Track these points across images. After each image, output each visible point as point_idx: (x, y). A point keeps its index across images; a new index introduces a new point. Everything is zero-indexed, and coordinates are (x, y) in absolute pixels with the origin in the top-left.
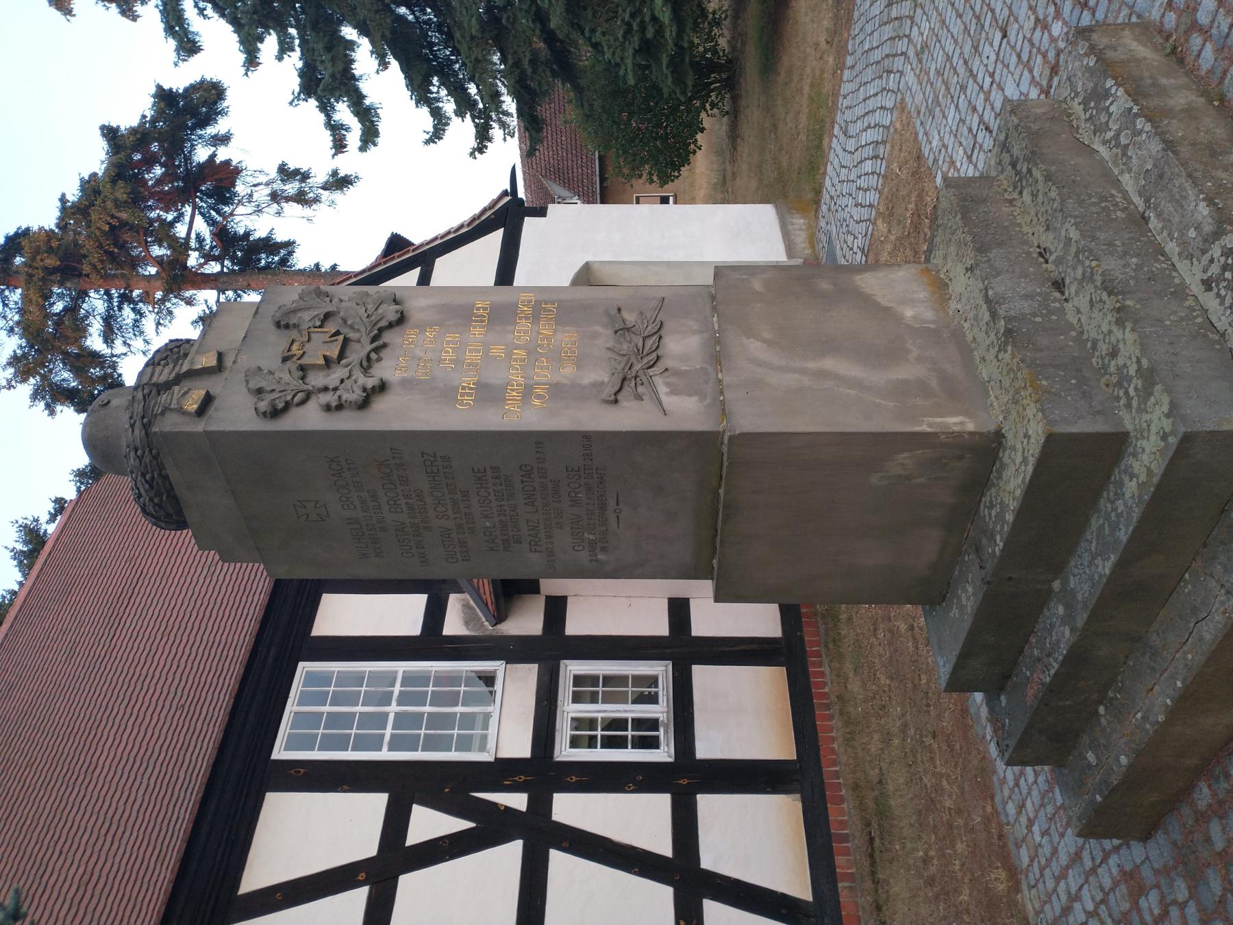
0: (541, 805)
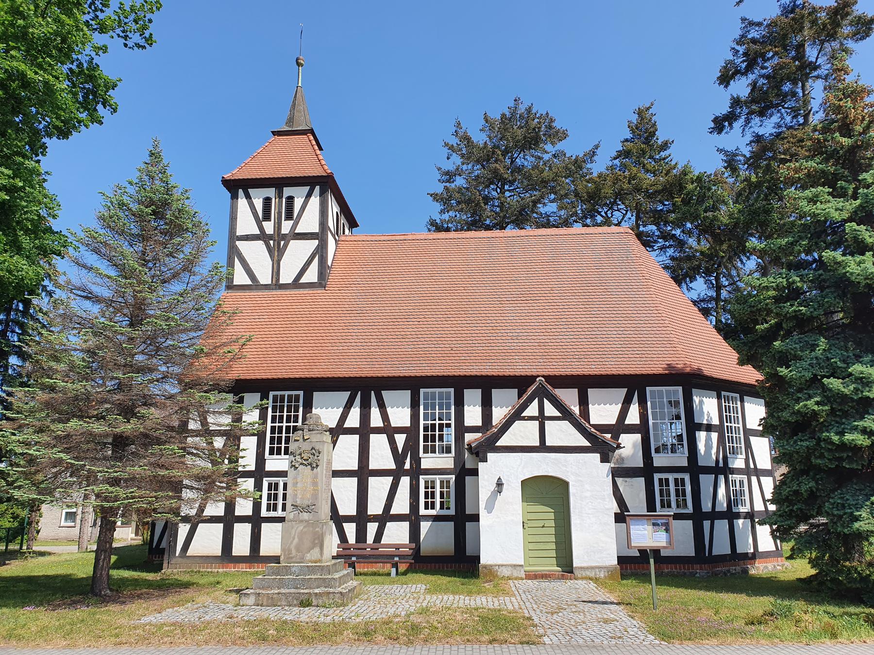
0: (406, 473)
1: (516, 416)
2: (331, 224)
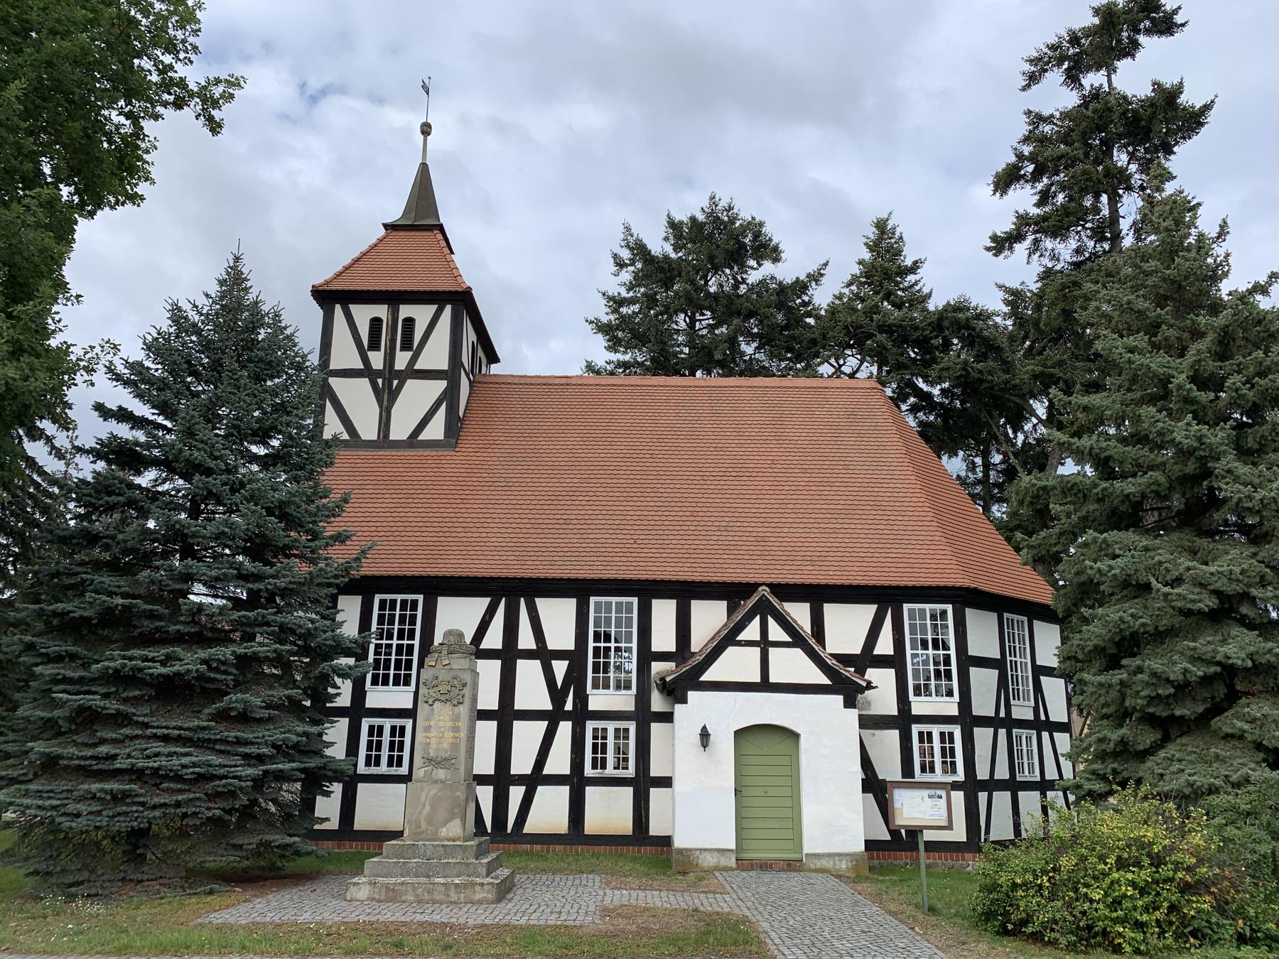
0: (567, 716)
1: (728, 639)
2: (466, 359)
